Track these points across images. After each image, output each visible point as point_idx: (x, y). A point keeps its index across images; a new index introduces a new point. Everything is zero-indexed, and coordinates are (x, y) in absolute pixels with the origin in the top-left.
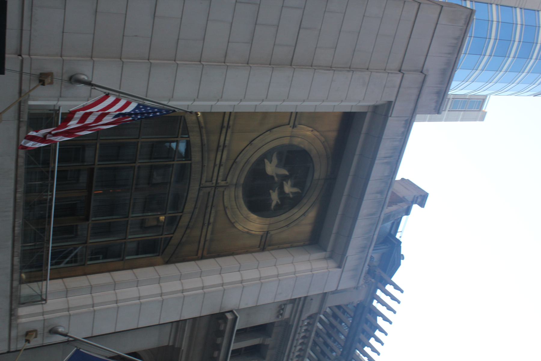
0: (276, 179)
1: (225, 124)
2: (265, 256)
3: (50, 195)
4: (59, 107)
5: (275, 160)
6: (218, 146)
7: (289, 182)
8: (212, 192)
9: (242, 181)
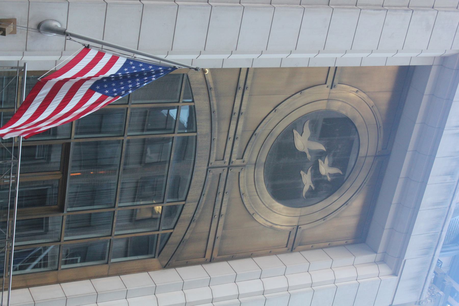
0: (309, 156)
1: (241, 84)
2: (294, 259)
3: (13, 179)
4: (25, 64)
5: (307, 131)
6: (232, 113)
7: (326, 160)
8: (225, 173)
9: (263, 159)
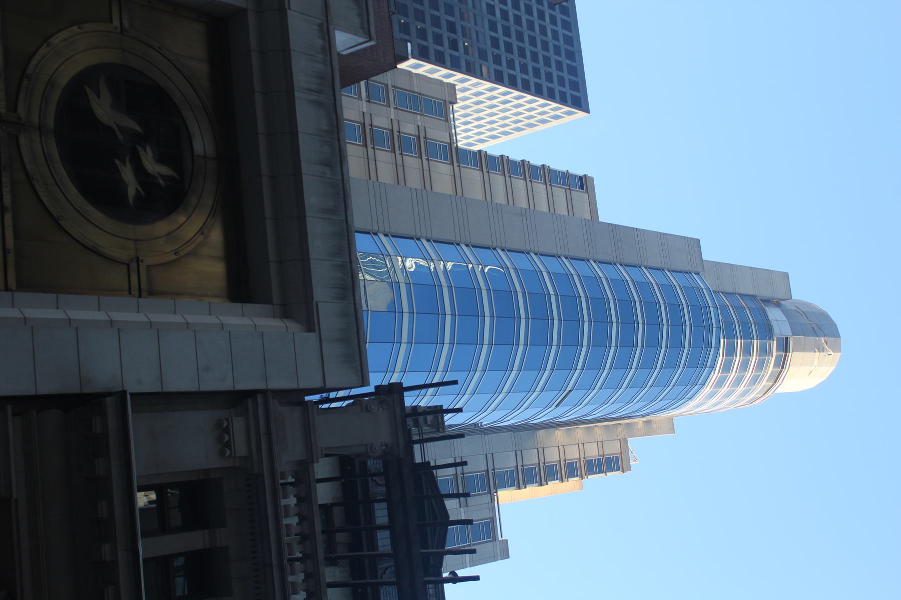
0: (120, 137)
9: (51, 123)
